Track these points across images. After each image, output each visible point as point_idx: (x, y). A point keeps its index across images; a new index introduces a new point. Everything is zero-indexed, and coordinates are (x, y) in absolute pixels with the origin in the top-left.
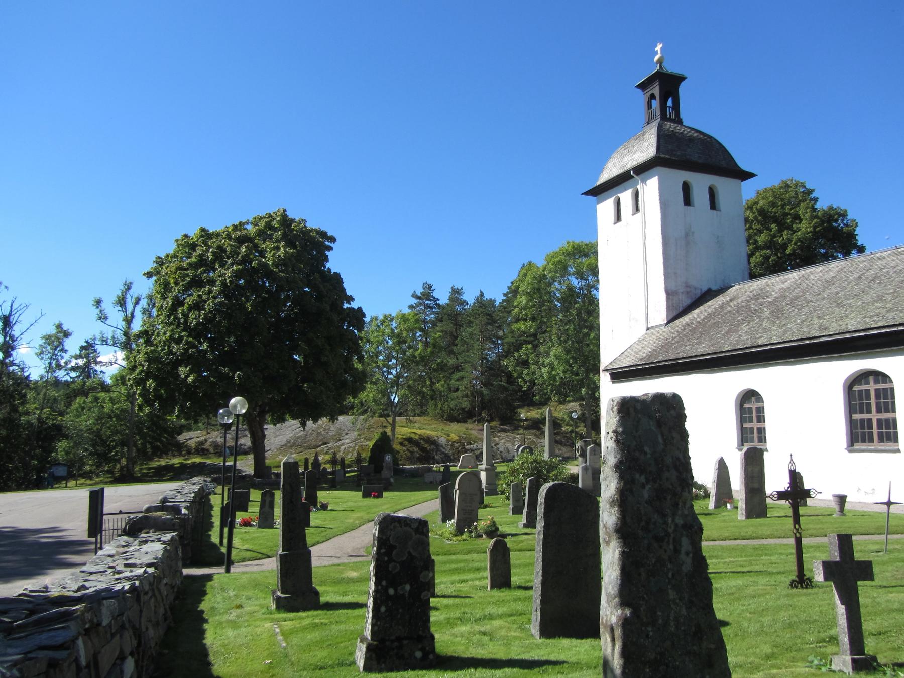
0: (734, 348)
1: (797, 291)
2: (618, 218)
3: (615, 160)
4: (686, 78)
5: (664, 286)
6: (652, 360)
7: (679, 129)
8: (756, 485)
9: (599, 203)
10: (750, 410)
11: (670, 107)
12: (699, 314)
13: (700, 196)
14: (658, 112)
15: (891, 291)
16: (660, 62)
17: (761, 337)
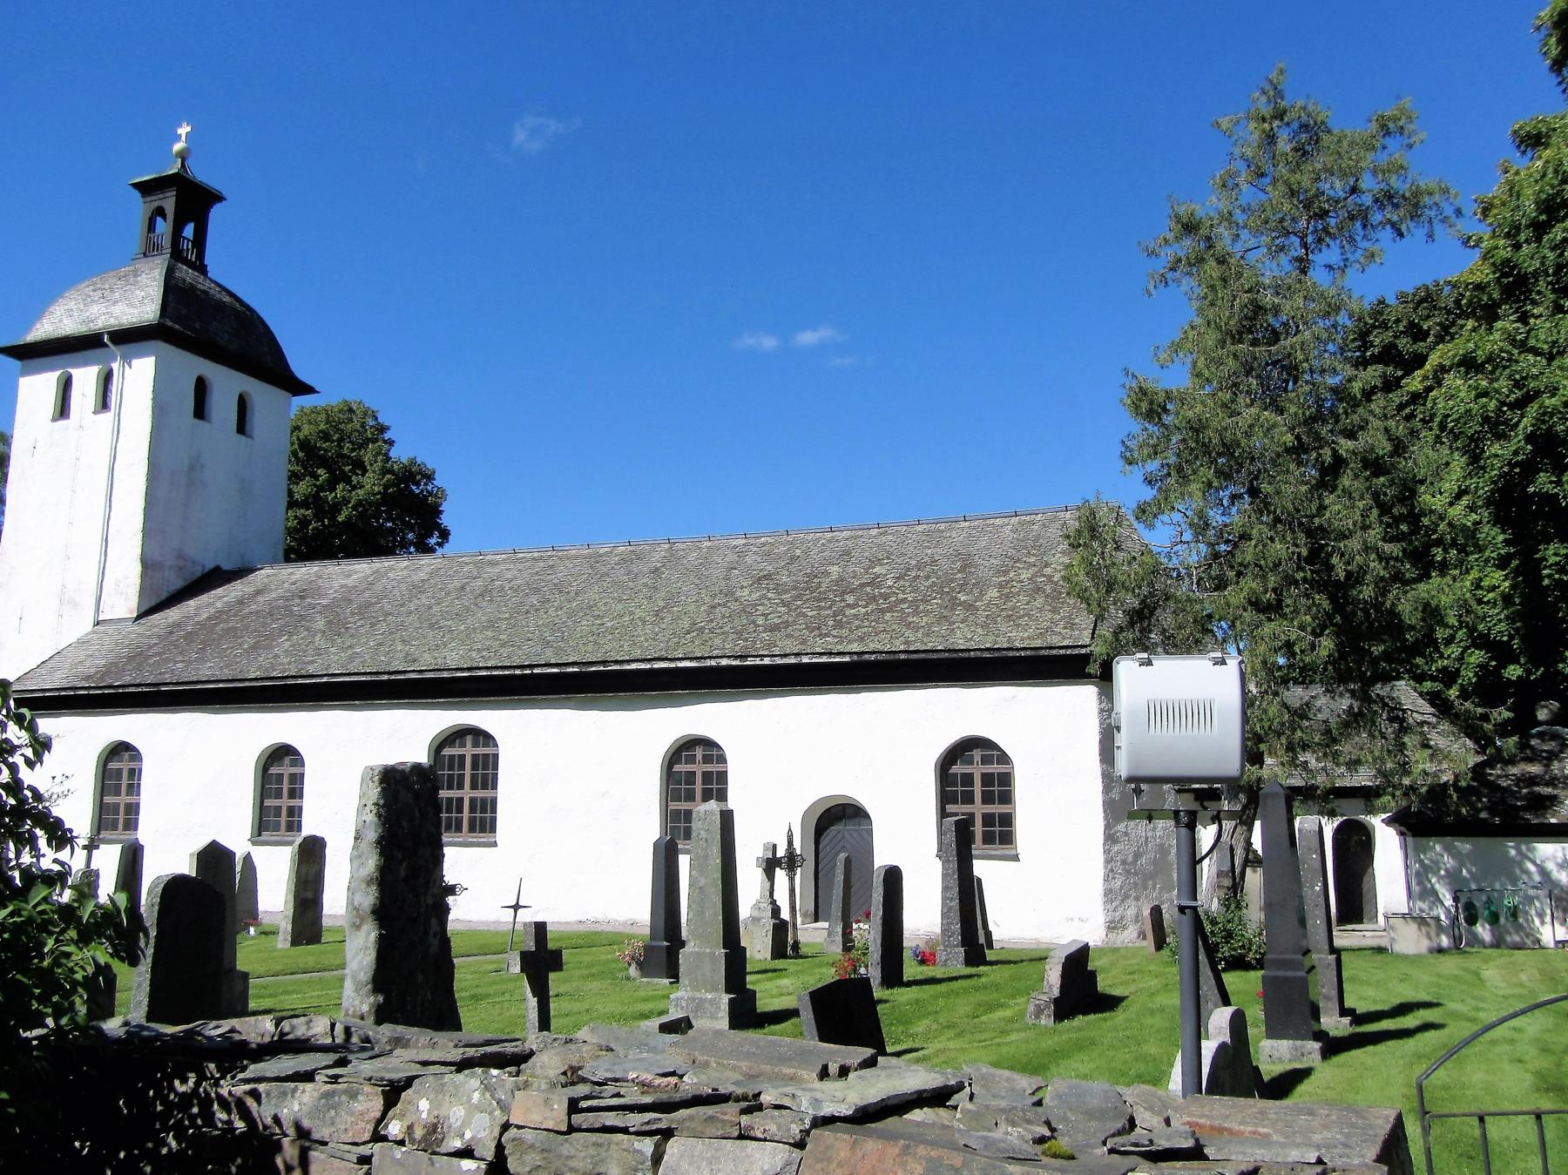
0: (266, 675)
1: (367, 594)
2: (63, 410)
3: (72, 305)
4: (225, 199)
5: (139, 551)
6: (109, 681)
7: (203, 284)
8: (310, 895)
9: (25, 373)
11: (188, 240)
12: (198, 608)
13: (223, 406)
14: (167, 242)
15: (507, 615)
16: (183, 155)
17: (312, 662)
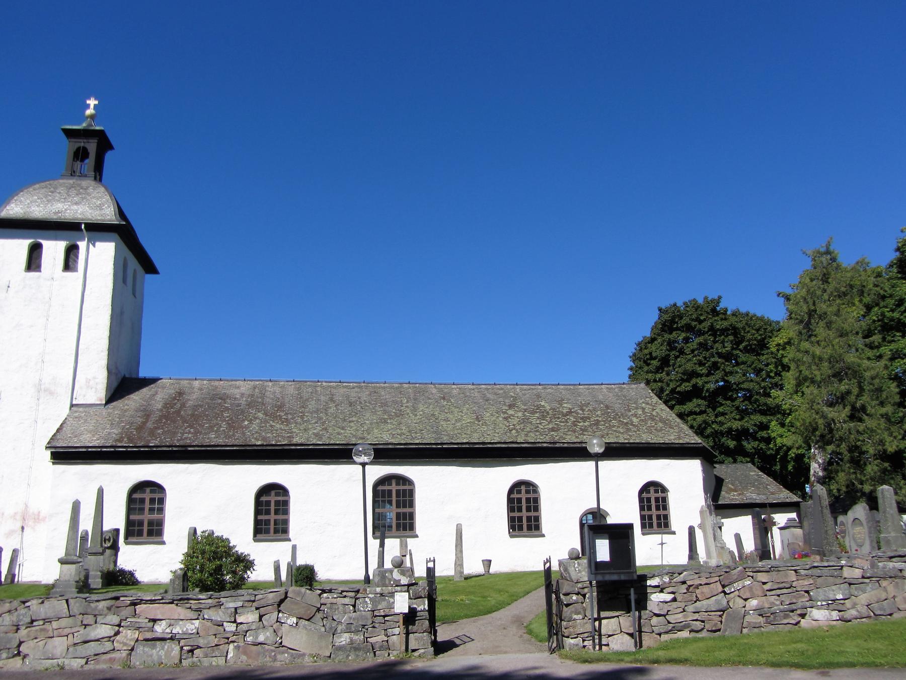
10: (268, 503)
